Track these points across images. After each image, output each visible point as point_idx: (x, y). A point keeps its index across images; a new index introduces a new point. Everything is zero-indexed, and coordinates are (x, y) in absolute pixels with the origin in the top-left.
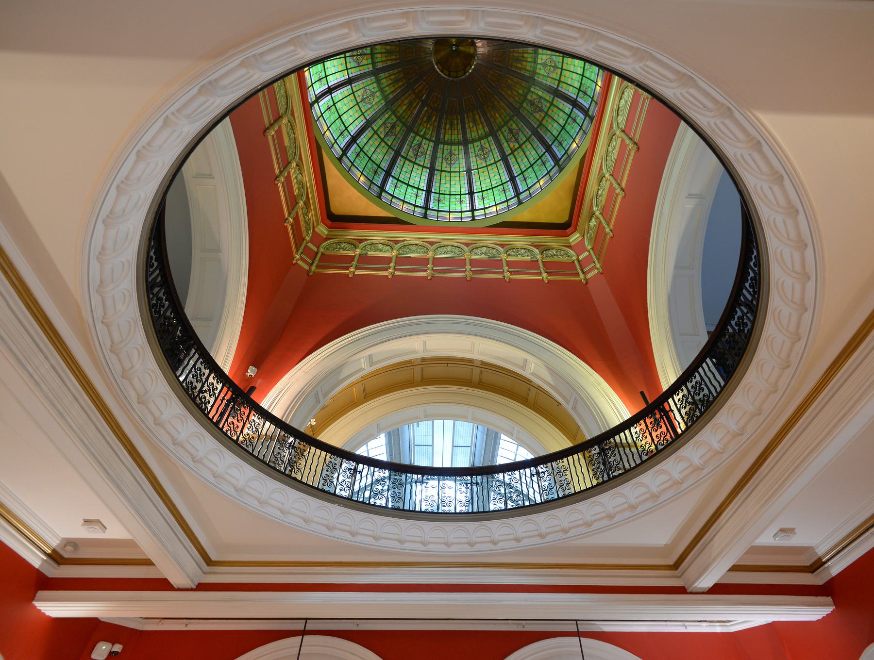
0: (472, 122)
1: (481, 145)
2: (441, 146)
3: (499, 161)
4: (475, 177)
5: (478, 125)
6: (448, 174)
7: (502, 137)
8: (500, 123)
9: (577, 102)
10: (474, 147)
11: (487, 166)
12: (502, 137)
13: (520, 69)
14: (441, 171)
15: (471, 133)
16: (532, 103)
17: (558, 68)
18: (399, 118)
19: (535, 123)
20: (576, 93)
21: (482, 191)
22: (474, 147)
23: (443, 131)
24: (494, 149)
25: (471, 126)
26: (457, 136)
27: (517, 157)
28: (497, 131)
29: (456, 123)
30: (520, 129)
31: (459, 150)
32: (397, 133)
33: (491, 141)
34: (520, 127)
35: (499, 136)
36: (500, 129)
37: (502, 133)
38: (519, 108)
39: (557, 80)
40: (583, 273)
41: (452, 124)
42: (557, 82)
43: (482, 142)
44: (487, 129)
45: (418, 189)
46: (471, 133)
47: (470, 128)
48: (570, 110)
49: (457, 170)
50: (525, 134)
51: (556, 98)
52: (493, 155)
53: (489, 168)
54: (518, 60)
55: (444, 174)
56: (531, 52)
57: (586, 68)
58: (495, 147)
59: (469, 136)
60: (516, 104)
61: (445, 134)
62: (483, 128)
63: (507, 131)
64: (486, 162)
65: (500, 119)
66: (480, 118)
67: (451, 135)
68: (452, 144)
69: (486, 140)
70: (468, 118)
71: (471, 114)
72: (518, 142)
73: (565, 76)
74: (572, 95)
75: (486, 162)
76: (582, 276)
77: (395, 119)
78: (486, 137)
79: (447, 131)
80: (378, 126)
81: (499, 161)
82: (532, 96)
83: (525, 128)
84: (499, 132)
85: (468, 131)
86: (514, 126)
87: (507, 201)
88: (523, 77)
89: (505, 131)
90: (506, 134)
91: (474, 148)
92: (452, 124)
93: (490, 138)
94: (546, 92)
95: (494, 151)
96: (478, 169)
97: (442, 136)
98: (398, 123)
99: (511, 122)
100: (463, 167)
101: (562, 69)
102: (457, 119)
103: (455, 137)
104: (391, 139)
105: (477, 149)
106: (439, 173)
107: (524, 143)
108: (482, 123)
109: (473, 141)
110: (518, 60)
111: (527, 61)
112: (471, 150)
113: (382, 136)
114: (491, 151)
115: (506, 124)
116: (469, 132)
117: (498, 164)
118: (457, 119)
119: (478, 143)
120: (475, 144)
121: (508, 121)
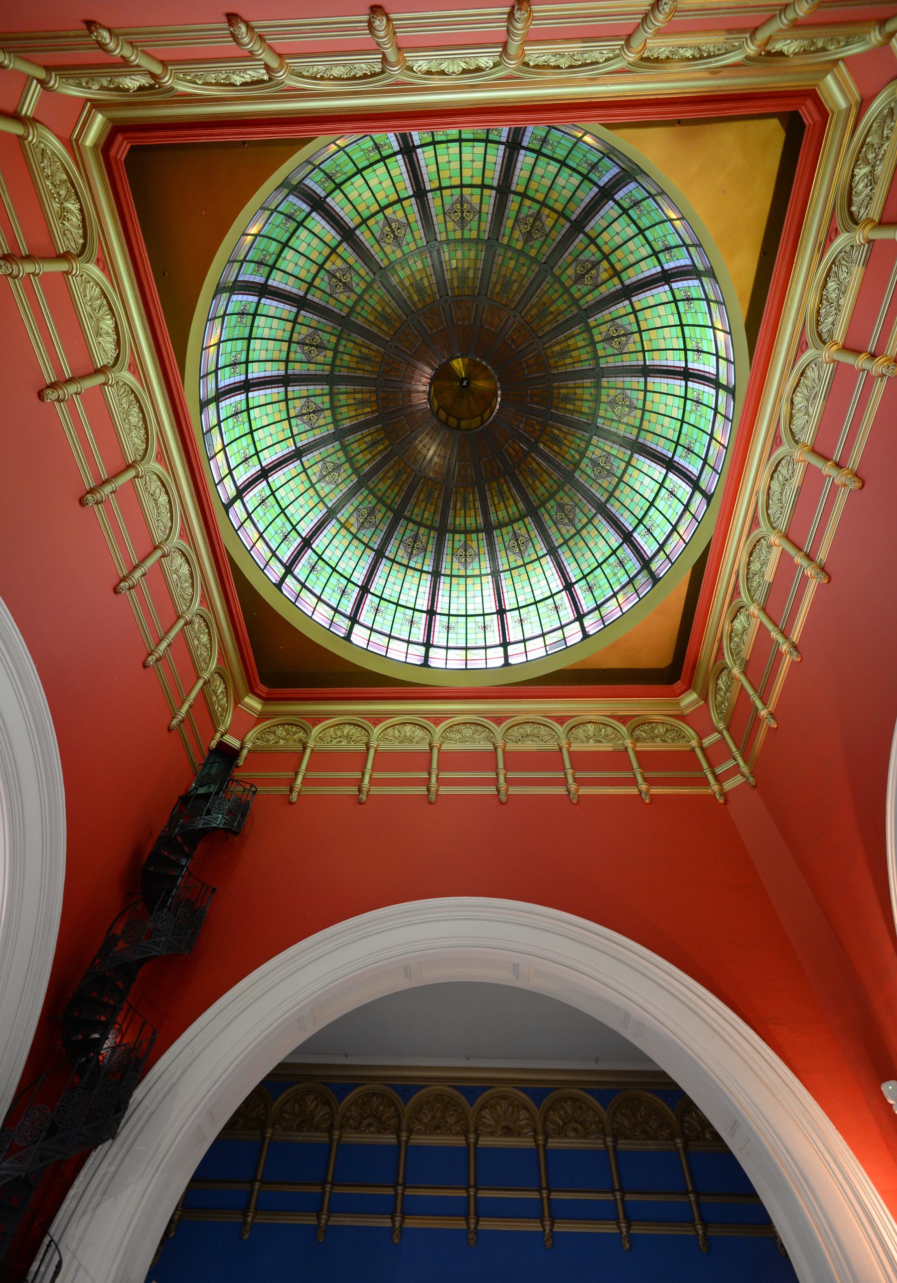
0: (497, 495)
1: (514, 532)
2: (449, 536)
3: (544, 556)
4: (506, 584)
5: (508, 499)
7: (546, 516)
8: (543, 494)
10: (502, 535)
11: (525, 565)
12: (546, 516)
13: (572, 412)
14: (451, 576)
15: (496, 512)
16: (595, 463)
17: (636, 408)
18: (380, 500)
19: (602, 495)
21: (519, 608)
22: (502, 535)
23: (451, 512)
25: (496, 502)
26: (473, 520)
27: (574, 549)
28: (539, 507)
30: (576, 505)
31: (479, 542)
32: (378, 522)
34: (577, 501)
35: (543, 515)
36: (543, 504)
37: (547, 512)
38: (574, 471)
39: (636, 427)
40: (717, 778)
41: (465, 502)
42: (635, 431)
43: (516, 526)
44: (521, 505)
45: (414, 609)
46: (496, 512)
48: (662, 476)
49: (477, 572)
50: (586, 511)
51: (636, 455)
53: (529, 567)
54: (567, 399)
56: (589, 385)
58: (537, 534)
59: (493, 517)
61: (455, 517)
62: (516, 504)
63: (555, 508)
64: (522, 558)
65: (543, 490)
66: (509, 490)
68: (466, 532)
69: (521, 523)
70: (490, 489)
71: (494, 484)
72: (574, 526)
75: (522, 558)
76: (715, 787)
77: (374, 501)
78: (521, 518)
79: (458, 512)
80: (347, 515)
81: (544, 556)
83: (585, 502)
84: (543, 510)
85: (492, 510)
88: (577, 425)
89: (552, 508)
90: (553, 512)
91: (502, 537)
92: (465, 502)
93: (528, 520)
94: (617, 447)
95: (535, 540)
96: (510, 570)
97: (450, 520)
98: (380, 506)
99: (561, 494)
100: (486, 568)
101: (644, 410)
103: (471, 521)
104: (369, 533)
105: (506, 538)
106: (447, 579)
107: (584, 526)
108: (513, 498)
109: (500, 526)
110: (567, 399)
111: (583, 400)
112: (498, 541)
113: (354, 530)
114: (531, 539)
115: (552, 496)
116: (494, 511)
117: (543, 560)
118: (474, 493)
119: (509, 528)
121: (556, 493)
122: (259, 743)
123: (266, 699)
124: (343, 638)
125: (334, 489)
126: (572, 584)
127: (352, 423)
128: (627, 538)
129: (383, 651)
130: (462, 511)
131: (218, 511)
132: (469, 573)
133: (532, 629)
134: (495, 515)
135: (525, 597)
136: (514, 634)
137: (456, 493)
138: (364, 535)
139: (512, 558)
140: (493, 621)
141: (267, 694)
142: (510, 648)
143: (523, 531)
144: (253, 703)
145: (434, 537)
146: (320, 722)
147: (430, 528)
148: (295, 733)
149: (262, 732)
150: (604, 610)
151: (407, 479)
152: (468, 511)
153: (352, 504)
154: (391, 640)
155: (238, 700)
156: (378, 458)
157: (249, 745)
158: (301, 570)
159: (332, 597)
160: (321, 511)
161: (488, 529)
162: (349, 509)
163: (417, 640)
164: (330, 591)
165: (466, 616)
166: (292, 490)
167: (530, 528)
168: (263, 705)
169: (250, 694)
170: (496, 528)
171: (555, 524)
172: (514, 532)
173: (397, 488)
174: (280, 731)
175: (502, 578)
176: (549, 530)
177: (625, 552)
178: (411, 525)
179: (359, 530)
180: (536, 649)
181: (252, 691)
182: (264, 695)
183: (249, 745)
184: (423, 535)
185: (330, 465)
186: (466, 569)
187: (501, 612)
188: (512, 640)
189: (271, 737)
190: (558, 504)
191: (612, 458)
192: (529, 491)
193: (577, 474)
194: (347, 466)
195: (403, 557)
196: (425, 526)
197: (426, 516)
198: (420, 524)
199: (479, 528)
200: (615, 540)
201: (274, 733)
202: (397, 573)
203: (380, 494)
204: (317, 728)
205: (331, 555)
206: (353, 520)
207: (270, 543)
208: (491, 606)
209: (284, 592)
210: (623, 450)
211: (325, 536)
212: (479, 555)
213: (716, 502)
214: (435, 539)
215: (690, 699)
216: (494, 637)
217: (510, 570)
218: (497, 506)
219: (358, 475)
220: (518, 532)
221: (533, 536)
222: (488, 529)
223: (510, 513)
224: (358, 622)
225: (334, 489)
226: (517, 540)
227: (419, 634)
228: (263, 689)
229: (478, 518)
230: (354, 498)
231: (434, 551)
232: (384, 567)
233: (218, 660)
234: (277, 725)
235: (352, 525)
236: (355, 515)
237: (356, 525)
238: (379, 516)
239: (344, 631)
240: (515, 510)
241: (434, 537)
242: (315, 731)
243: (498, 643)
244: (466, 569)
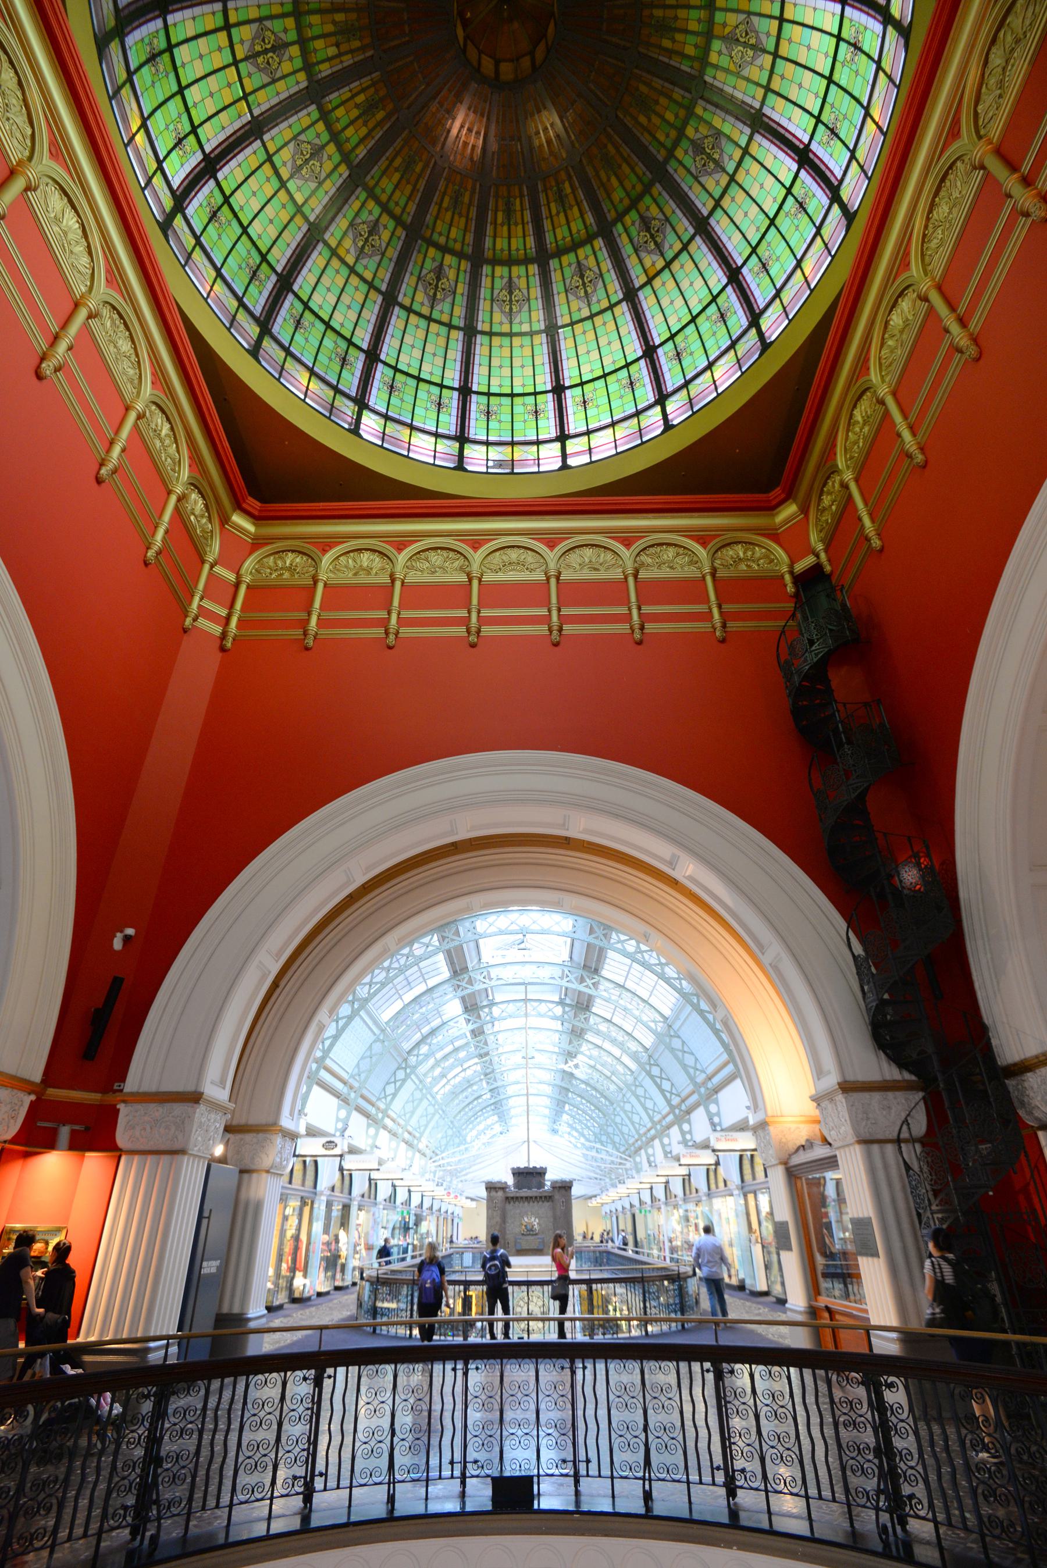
1: (578, 262)
2: (487, 269)
3: (619, 302)
6: (506, 341)
9: (811, 155)
12: (625, 238)
13: (670, 53)
14: (491, 334)
15: (554, 229)
17: (765, 51)
18: (385, 208)
20: (810, 130)
23: (489, 230)
24: (608, 271)
25: (554, 211)
26: (523, 242)
28: (614, 223)
29: (518, 207)
31: (527, 278)
32: (384, 245)
33: (600, 249)
34: (668, 213)
35: (620, 235)
36: (620, 217)
37: (626, 230)
38: (667, 160)
41: (509, 212)
44: (590, 219)
46: (554, 229)
47: (551, 217)
48: (792, 175)
52: (605, 286)
55: (496, 341)
57: (840, 57)
59: (549, 238)
60: (659, 151)
61: (495, 237)
66: (573, 190)
67: (509, 238)
68: (510, 262)
69: (588, 249)
70: (545, 190)
73: (782, 77)
74: (799, 134)
75: (589, 305)
77: (377, 211)
79: (499, 227)
80: (338, 235)
82: (697, 130)
84: (619, 226)
85: (547, 225)
86: (654, 211)
87: (638, 413)
88: (675, 77)
90: (634, 232)
91: (562, 270)
92: (509, 212)
94: (732, 120)
95: (606, 276)
96: (572, 324)
97: (488, 243)
102: (522, 196)
104: (372, 264)
105: (568, 272)
106: (485, 339)
107: (676, 256)
108: (579, 204)
109: (560, 253)
111: (686, 32)
112: (556, 277)
113: (350, 260)
114: (601, 275)
115: (634, 204)
116: (550, 228)
117: (617, 310)
118: (522, 196)
120: (565, 259)
123: (256, 518)
124: (349, 430)
125: (317, 188)
126: (655, 348)
127: (335, 69)
128: (734, 276)
129: (403, 448)
130: (505, 228)
131: (154, 234)
132: (516, 329)
133: (599, 416)
134: (551, 233)
135: (591, 368)
136: (575, 423)
137: (497, 196)
138: (366, 267)
139: (575, 304)
140: (547, 403)
141: (260, 511)
142: (568, 443)
143: (591, 262)
145: (465, 271)
146: (331, 548)
147: (460, 255)
150: (694, 388)
151: (423, 170)
152: (513, 227)
153: (345, 216)
154: (413, 433)
155: (224, 520)
156: (378, 134)
158: (282, 327)
159: (328, 367)
160: (299, 228)
161: (542, 257)
162: (342, 224)
163: (447, 432)
164: (325, 361)
165: (512, 395)
166: (254, 194)
167: (600, 258)
169: (238, 511)
170: (553, 256)
171: (636, 251)
172: (578, 262)
173: (409, 188)
175: (561, 337)
176: (627, 261)
177: (731, 299)
178: (432, 251)
179: (357, 259)
180: (604, 445)
182: (256, 513)
183: (247, 579)
184: (450, 267)
185: (307, 148)
186: (511, 323)
187: (559, 390)
188: (572, 432)
190: (642, 218)
191: (724, 141)
192: (601, 194)
193: (672, 166)
194: (331, 148)
195: (422, 304)
196: (453, 252)
197: (453, 235)
198: (444, 249)
199: (529, 256)
200: (717, 278)
202: (416, 328)
203: (384, 198)
204: (328, 555)
205: (322, 302)
206: (348, 243)
207: (233, 285)
208: (545, 382)
209: (263, 363)
210: (740, 125)
211: (310, 271)
212: (529, 300)
213: (860, 223)
214: (468, 274)
215: (790, 510)
216: (548, 428)
217: (572, 324)
218: (555, 219)
219: (350, 166)
220: (584, 262)
221: (604, 269)
222: (542, 257)
223: (574, 231)
224: (367, 407)
225: (317, 188)
226: (582, 277)
227: (449, 423)
229: (527, 238)
230: (347, 206)
231: (466, 293)
232: (397, 319)
233: (190, 466)
235: (348, 251)
236: (350, 234)
237: (352, 251)
238: (386, 235)
239: (349, 420)
240: (581, 226)
241: (465, 271)
242: (327, 559)
243: (553, 435)
244: (511, 323)
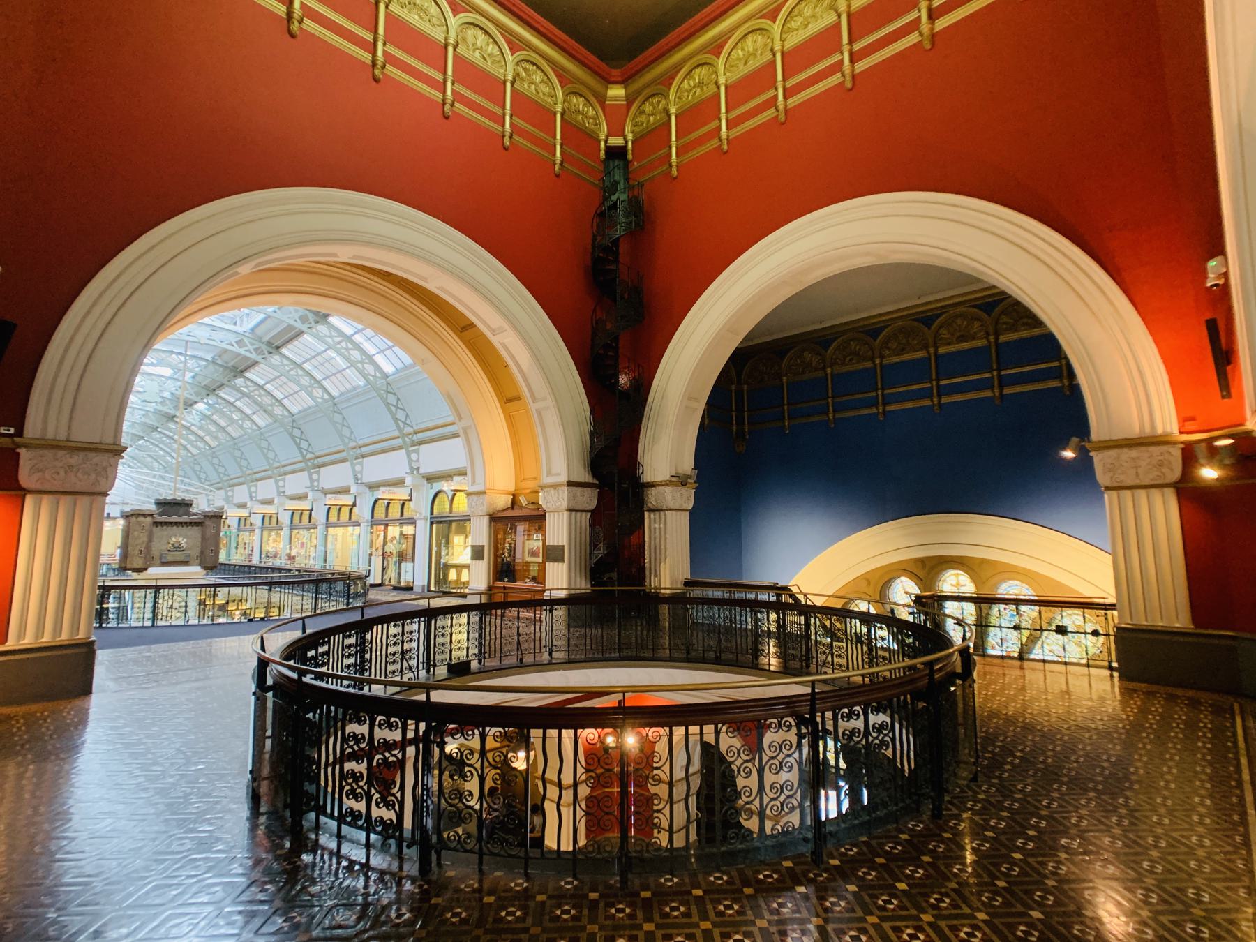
122: (637, 129)
123: (624, 82)
144: (616, 92)
148: (659, 102)
149: (635, 116)
157: (630, 137)
168: (625, 88)
169: (610, 86)
174: (648, 108)
181: (608, 81)
182: (620, 79)
183: (630, 137)
189: (643, 118)
201: (643, 112)
228: (616, 73)
234: (643, 103)
